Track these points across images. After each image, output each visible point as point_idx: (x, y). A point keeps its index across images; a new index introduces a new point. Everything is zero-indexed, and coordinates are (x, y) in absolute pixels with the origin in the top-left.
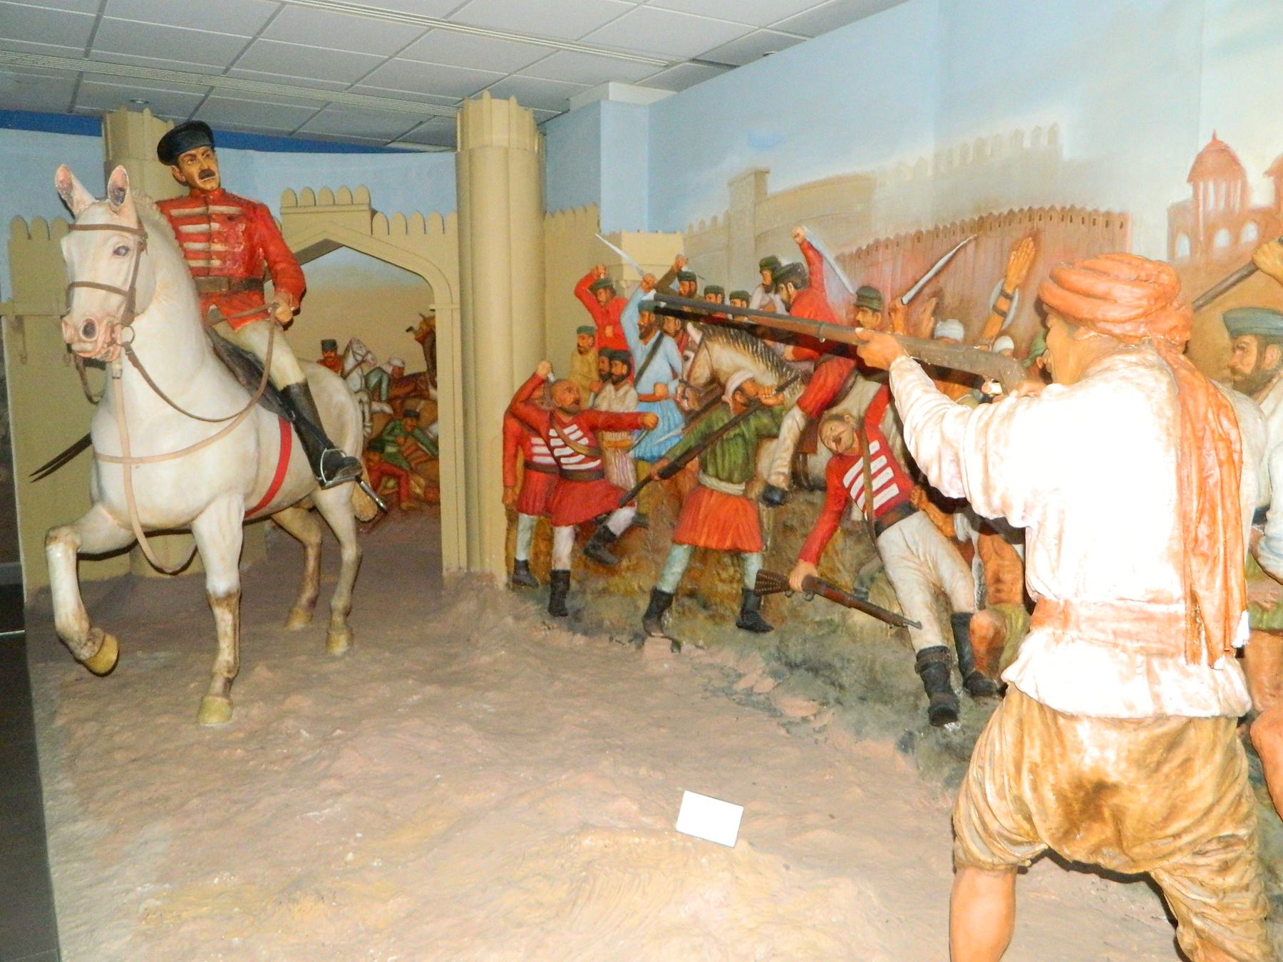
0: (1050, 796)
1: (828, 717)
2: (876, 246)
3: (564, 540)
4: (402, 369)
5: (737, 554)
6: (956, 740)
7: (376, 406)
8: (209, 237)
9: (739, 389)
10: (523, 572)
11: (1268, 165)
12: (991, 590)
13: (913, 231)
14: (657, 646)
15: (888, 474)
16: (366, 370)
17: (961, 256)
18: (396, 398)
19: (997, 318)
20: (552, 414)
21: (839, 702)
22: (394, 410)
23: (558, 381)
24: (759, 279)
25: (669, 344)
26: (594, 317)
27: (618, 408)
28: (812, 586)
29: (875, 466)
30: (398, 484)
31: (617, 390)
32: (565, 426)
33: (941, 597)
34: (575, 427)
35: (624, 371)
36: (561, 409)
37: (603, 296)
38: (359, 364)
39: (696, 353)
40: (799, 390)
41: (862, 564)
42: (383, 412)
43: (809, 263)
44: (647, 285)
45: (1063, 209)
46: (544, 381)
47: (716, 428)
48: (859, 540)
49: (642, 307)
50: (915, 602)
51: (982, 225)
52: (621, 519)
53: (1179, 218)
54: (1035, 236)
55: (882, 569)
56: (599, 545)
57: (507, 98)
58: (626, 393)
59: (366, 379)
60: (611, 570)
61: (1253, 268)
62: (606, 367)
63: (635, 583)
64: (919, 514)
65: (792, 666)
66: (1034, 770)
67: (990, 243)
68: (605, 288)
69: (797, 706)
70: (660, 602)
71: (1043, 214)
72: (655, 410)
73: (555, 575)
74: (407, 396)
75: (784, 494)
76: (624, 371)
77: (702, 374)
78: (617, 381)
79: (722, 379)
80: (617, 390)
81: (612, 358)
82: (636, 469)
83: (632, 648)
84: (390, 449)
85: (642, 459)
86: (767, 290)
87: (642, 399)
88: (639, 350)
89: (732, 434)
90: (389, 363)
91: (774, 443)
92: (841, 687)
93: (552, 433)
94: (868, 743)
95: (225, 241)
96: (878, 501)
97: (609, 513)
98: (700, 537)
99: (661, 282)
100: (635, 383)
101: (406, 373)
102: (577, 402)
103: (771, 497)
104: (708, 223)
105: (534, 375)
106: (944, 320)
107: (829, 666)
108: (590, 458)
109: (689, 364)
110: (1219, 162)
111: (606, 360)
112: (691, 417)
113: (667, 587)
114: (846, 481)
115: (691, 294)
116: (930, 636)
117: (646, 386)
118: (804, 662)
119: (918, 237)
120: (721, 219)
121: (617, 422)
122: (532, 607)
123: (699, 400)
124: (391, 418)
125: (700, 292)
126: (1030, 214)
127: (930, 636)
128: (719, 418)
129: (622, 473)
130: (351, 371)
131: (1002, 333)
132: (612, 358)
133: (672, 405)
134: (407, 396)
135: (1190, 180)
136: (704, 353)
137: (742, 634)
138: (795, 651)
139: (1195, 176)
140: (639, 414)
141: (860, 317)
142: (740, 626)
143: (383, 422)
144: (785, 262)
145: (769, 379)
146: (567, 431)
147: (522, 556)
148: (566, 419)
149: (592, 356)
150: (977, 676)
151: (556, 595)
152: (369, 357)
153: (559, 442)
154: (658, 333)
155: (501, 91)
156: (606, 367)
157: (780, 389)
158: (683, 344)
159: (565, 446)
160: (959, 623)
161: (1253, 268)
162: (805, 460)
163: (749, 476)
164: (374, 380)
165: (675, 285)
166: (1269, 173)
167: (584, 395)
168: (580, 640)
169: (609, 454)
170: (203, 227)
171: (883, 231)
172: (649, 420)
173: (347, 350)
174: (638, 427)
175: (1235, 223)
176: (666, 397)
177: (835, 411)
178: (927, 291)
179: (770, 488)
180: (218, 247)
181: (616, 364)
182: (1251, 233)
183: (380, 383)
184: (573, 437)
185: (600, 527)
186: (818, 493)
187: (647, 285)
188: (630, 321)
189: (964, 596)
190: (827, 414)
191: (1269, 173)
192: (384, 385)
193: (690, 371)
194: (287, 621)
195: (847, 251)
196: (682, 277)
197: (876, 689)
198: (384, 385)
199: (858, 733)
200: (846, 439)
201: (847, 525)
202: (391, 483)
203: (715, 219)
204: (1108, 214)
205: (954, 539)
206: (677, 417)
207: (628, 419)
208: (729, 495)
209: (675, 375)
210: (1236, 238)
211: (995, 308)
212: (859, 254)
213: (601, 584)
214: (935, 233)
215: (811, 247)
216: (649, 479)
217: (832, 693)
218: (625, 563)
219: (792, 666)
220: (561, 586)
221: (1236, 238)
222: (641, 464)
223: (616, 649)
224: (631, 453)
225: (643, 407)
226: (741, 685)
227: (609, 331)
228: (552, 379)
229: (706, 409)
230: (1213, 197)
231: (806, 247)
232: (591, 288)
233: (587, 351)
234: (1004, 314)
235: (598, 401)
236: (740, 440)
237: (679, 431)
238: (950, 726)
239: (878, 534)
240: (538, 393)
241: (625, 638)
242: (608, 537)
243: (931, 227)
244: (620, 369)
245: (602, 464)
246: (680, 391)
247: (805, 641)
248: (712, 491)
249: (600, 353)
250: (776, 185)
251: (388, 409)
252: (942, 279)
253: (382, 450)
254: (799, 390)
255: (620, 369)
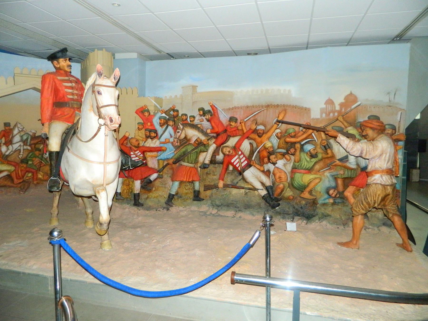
0: (380, 198)
1: (240, 214)
2: (235, 108)
3: (137, 185)
4: (35, 133)
5: (192, 182)
6: (279, 210)
7: (25, 147)
8: (72, 88)
9: (196, 140)
10: (119, 197)
11: (338, 104)
12: (278, 180)
13: (246, 105)
14: (174, 210)
15: (244, 158)
16: (22, 133)
17: (262, 112)
18: (33, 144)
19: (276, 125)
20: (130, 148)
21: (239, 210)
22: (32, 148)
23: (132, 138)
24: (198, 113)
25: (170, 129)
26: (143, 120)
27: (152, 145)
28: (226, 186)
29: (241, 157)
30: (33, 174)
31: (152, 141)
32: (135, 151)
33: (263, 184)
34: (138, 151)
35: (155, 135)
36: (134, 146)
37: (146, 114)
38: (20, 132)
39: (182, 131)
40: (214, 140)
41: (233, 180)
42: (28, 149)
43: (213, 109)
44: (163, 112)
45: (293, 106)
46: (127, 138)
47: (189, 151)
48: (232, 175)
49: (160, 118)
50: (258, 185)
51: (268, 106)
52: (154, 176)
53: (322, 111)
54: (285, 110)
55: (244, 179)
56: (147, 185)
57: (110, 52)
58: (156, 142)
59: (22, 137)
60: (150, 191)
61: (337, 119)
62: (148, 134)
63: (159, 194)
64: (253, 167)
65: (218, 206)
66: (379, 195)
67: (271, 110)
68: (148, 112)
69: (230, 213)
70: (171, 197)
71: (287, 106)
72: (165, 145)
73: (135, 195)
74: (37, 143)
75: (209, 165)
76: (155, 135)
77: (183, 136)
78: (152, 138)
79: (188, 138)
80: (152, 141)
81: (150, 131)
82: (158, 162)
83: (165, 210)
84: (30, 162)
85: (161, 159)
86: (201, 116)
87: (161, 143)
88: (160, 130)
89: (194, 151)
90: (31, 132)
91: (205, 153)
92: (238, 207)
93: (132, 153)
94: (256, 216)
95: (77, 90)
96: (243, 165)
97: (150, 175)
98: (184, 178)
99: (167, 111)
100: (159, 139)
101: (37, 135)
102: (139, 144)
103: (204, 166)
104: (173, 97)
105: (124, 136)
106: (259, 125)
107: (233, 204)
108: (144, 160)
109: (179, 134)
110: (330, 102)
111: (148, 132)
112: (177, 148)
113: (173, 193)
114: (232, 161)
115: (178, 115)
116: (264, 192)
117: (163, 139)
118: (222, 205)
119: (247, 107)
120: (179, 96)
121: (151, 150)
122: (128, 206)
123: (180, 143)
124: (31, 151)
125: (180, 115)
126: (284, 106)
127: (264, 192)
128: (190, 148)
129: (152, 163)
130: (17, 134)
131: (276, 129)
132: (150, 131)
133: (170, 145)
134: (37, 143)
135: (325, 104)
136: (184, 131)
137: (195, 202)
138: (218, 203)
139: (325, 103)
140: (161, 147)
141: (231, 123)
142: (194, 200)
143: (27, 153)
144: (206, 109)
145: (203, 138)
146: (136, 152)
147: (119, 191)
148: (135, 149)
149: (143, 131)
150: (276, 198)
151: (136, 201)
152: (24, 129)
153: (134, 156)
154: (166, 125)
155: (108, 50)
156: (148, 134)
157: (208, 140)
158: (176, 129)
159: (136, 157)
160: (267, 188)
161: (337, 119)
162: (215, 157)
163: (196, 162)
164: (25, 138)
165: (172, 113)
166: (339, 105)
167: (141, 142)
168: (147, 212)
169: (149, 159)
170: (70, 84)
171: (236, 104)
172: (163, 148)
173: (15, 126)
174: (160, 151)
175: (333, 112)
176: (169, 142)
177: (224, 145)
178: (252, 119)
179: (206, 164)
180: (76, 92)
181: (152, 134)
182: (336, 114)
183: (27, 139)
184: (138, 154)
185: (146, 180)
186: (217, 165)
187: (163, 112)
188: (156, 121)
189: (268, 183)
190: (222, 146)
191: (339, 105)
192: (29, 140)
193: (180, 136)
194: (50, 223)
195: (226, 108)
196: (174, 110)
197: (247, 206)
198: (29, 140)
199: (253, 215)
200: (231, 151)
201: (228, 172)
202: (30, 175)
203: (176, 96)
204: (306, 108)
205: (263, 171)
206: (172, 147)
207: (158, 149)
208: (190, 167)
209: (171, 137)
210: (334, 115)
211: (275, 123)
212: (229, 109)
213: (146, 196)
214: (253, 106)
215: (214, 106)
216: (168, 164)
217: (237, 209)
218: (154, 189)
219: (218, 206)
220: (137, 197)
221: (334, 115)
222: (160, 161)
223: (160, 212)
224: (157, 158)
225: (162, 145)
226: (208, 213)
227: (149, 124)
228: (130, 138)
229: (181, 145)
230: (330, 108)
231: (212, 106)
232: (142, 112)
233: (141, 129)
234: (278, 125)
235: (145, 144)
236: (196, 153)
237: (173, 152)
238: (277, 208)
239: (244, 172)
240: (125, 142)
241: (161, 210)
242: (150, 182)
243: (252, 105)
244: (153, 134)
245: (146, 162)
246: (176, 140)
247: (220, 200)
248: (186, 166)
249: (146, 130)
250: (199, 90)
251: (29, 148)
252: (256, 117)
253: (27, 163)
254: (214, 140)
255: (153, 134)
